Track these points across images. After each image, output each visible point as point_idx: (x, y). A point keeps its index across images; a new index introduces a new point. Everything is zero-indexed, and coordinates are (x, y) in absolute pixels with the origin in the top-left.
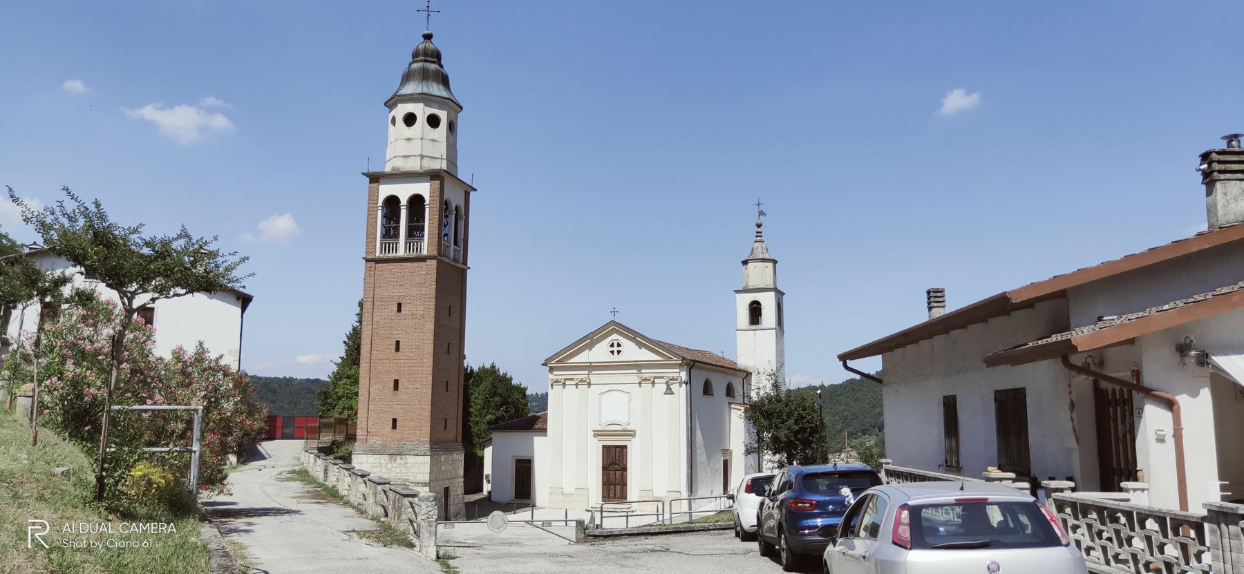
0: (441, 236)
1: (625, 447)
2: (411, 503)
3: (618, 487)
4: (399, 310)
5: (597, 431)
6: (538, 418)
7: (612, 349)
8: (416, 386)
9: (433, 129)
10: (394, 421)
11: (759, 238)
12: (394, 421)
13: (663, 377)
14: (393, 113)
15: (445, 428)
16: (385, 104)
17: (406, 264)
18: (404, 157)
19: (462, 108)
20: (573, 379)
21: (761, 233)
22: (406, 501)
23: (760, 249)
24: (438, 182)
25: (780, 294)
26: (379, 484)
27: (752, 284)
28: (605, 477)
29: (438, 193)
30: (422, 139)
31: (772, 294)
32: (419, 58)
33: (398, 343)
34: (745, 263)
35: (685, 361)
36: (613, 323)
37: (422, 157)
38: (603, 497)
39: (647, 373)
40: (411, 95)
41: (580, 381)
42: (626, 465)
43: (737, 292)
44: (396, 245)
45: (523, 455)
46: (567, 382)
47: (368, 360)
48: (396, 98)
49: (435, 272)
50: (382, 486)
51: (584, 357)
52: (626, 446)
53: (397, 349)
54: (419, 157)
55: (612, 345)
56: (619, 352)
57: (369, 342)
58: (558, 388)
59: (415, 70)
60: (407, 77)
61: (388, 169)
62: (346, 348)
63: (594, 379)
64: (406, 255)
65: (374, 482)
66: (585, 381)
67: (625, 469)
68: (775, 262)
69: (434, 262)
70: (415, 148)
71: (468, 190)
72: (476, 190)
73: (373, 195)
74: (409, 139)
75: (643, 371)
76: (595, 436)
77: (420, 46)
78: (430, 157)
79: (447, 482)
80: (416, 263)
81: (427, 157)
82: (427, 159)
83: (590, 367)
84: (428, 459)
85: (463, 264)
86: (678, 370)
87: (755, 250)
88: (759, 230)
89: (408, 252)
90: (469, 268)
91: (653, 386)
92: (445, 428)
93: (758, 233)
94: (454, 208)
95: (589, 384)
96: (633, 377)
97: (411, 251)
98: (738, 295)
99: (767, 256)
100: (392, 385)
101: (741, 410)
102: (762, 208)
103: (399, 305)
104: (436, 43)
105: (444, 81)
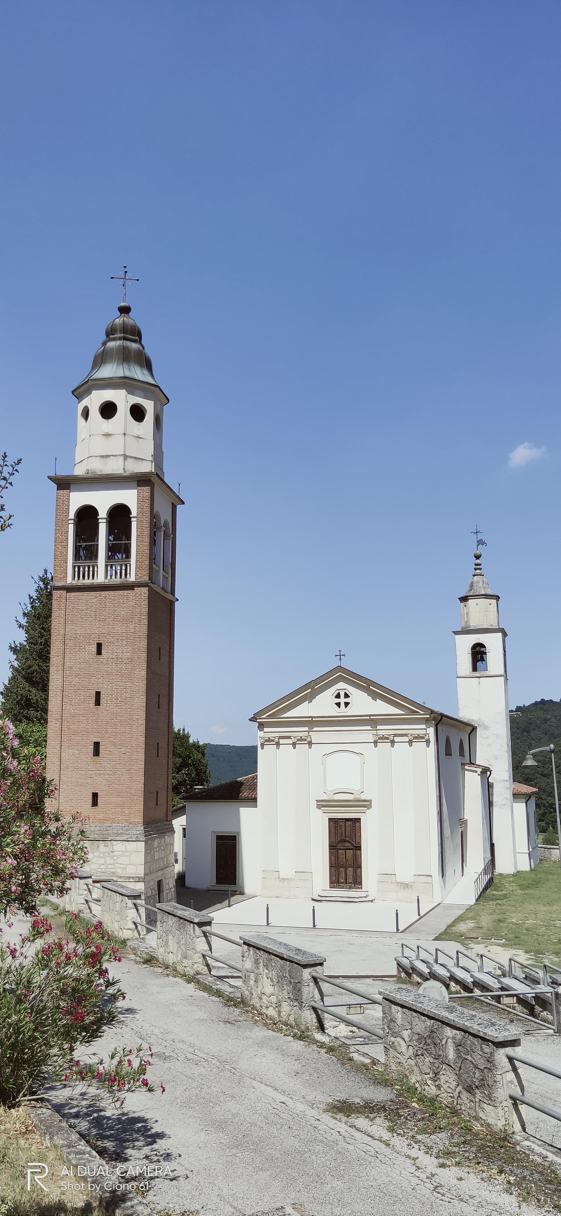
0: (152, 559)
1: (358, 820)
2: (511, 1059)
3: (350, 870)
4: (99, 652)
5: (322, 801)
6: (241, 784)
7: (338, 700)
8: (123, 750)
9: (137, 423)
10: (95, 796)
11: (478, 571)
12: (95, 796)
13: (406, 735)
14: (85, 402)
15: (157, 804)
16: (73, 392)
17: (107, 593)
18: (102, 457)
19: (168, 400)
20: (289, 737)
21: (480, 565)
22: (501, 1055)
23: (481, 584)
24: (146, 490)
25: (505, 635)
26: (305, 966)
27: (474, 623)
28: (333, 858)
29: (147, 504)
30: (125, 434)
31: (500, 635)
32: (116, 336)
33: (98, 694)
34: (464, 599)
35: (433, 715)
36: (340, 668)
37: (126, 457)
38: (331, 882)
39: (384, 730)
40: (111, 378)
41: (298, 740)
42: (360, 843)
43: (456, 633)
44: (93, 569)
45: (226, 829)
46: (282, 741)
47: (58, 717)
48: (90, 383)
49: (146, 602)
50: (309, 970)
51: (303, 710)
52: (360, 819)
53: (98, 703)
54: (122, 458)
55: (338, 696)
56: (347, 704)
57: (59, 693)
58: (270, 748)
59: (112, 350)
60: (100, 359)
61: (79, 471)
62: (3, 700)
63: (315, 737)
64: (106, 581)
65: (282, 958)
66: (305, 740)
67: (359, 848)
68: (497, 598)
69: (145, 590)
70: (116, 446)
71: (176, 501)
72: (183, 503)
73: (62, 506)
74: (107, 435)
75: (379, 727)
76: (319, 807)
77: (117, 320)
78: (135, 458)
79: (160, 873)
80: (121, 592)
81: (131, 457)
82: (132, 459)
83: (311, 723)
84: (141, 846)
85: (171, 594)
86: (424, 726)
87: (475, 585)
88: (478, 561)
89: (109, 577)
90: (178, 600)
91: (393, 746)
92: (157, 804)
93: (476, 565)
94: (162, 525)
95: (310, 743)
96: (367, 734)
97: (114, 577)
98: (458, 637)
99: (489, 592)
100: (91, 748)
101: (476, 772)
102: (480, 536)
103: (99, 646)
104: (134, 319)
105: (147, 365)
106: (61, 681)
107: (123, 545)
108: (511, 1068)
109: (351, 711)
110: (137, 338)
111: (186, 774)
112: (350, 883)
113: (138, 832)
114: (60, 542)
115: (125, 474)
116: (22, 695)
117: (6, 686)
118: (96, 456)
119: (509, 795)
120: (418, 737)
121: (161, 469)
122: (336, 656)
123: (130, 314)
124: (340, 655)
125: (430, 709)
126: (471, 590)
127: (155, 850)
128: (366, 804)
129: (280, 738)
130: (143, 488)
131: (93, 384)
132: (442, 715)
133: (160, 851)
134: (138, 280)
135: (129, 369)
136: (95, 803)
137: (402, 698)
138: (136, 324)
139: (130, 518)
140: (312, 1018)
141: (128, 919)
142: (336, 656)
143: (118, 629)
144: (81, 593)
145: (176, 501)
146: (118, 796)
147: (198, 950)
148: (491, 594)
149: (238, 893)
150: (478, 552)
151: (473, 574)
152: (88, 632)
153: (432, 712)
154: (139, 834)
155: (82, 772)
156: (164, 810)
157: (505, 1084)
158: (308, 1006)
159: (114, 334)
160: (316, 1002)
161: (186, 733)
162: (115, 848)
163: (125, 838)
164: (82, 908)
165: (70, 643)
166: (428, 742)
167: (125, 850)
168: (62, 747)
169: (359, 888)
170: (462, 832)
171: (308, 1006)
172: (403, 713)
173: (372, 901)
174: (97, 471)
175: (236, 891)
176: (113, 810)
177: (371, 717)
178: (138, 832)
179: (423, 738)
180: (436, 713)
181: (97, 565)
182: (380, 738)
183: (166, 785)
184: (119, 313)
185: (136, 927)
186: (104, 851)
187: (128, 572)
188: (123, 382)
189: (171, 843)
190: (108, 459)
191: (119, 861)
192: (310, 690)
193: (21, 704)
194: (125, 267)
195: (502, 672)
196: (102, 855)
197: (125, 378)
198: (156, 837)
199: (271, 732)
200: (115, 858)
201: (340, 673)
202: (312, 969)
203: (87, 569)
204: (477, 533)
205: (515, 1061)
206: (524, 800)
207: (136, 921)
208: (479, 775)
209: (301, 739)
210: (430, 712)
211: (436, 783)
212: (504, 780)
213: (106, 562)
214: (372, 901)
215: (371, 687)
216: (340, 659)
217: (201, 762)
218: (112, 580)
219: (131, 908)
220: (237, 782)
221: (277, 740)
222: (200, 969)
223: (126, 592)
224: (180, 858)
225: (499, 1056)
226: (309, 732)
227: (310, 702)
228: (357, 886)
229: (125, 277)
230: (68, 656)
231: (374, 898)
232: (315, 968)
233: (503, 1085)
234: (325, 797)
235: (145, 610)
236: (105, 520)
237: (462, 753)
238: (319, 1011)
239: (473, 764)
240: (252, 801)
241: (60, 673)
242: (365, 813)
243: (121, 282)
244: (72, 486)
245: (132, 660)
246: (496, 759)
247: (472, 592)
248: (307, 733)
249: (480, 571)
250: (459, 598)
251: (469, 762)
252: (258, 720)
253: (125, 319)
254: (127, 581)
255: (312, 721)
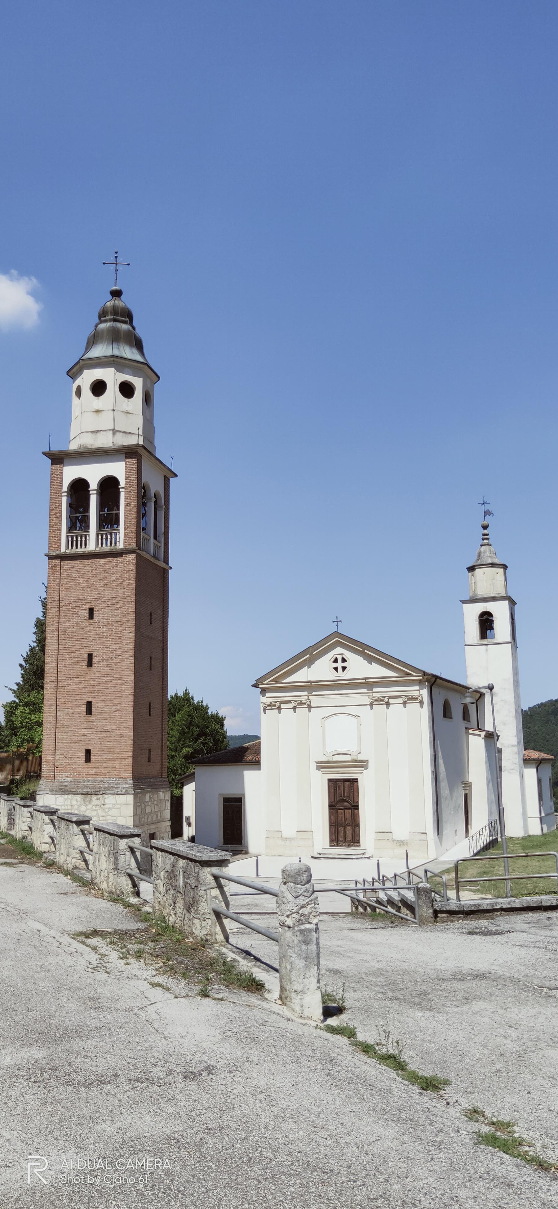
1: (356, 780)
2: (216, 878)
3: (349, 829)
4: (91, 616)
5: (321, 762)
7: (335, 665)
8: (113, 709)
9: (126, 399)
10: (88, 752)
11: (485, 541)
12: (88, 752)
13: (400, 697)
14: (78, 382)
15: (149, 761)
16: (68, 373)
17: (98, 560)
18: (93, 432)
19: (159, 377)
20: (289, 702)
21: (487, 535)
22: (207, 874)
23: (488, 553)
24: (133, 462)
25: (512, 603)
26: (122, 837)
27: (481, 592)
28: (332, 817)
29: (134, 475)
30: (114, 410)
31: (506, 603)
32: (107, 318)
33: (90, 656)
34: (471, 569)
35: (426, 677)
36: (336, 634)
37: (115, 431)
38: (331, 841)
39: (380, 692)
40: (100, 358)
41: (298, 704)
42: (358, 802)
43: (464, 602)
44: (86, 538)
45: (231, 792)
46: (283, 706)
47: (54, 678)
48: (81, 363)
49: (134, 568)
50: (125, 841)
51: (302, 675)
52: (357, 779)
53: (90, 664)
54: (111, 432)
55: (336, 661)
56: (344, 668)
57: (55, 656)
58: (272, 713)
59: (103, 331)
60: (93, 340)
61: (73, 446)
62: (22, 672)
63: (315, 701)
64: (97, 549)
65: (111, 834)
66: (305, 704)
67: (356, 807)
68: (505, 567)
69: (132, 557)
70: (106, 422)
71: (168, 475)
72: (176, 476)
73: (57, 479)
74: (98, 411)
75: (374, 690)
76: (319, 768)
77: (109, 303)
78: (124, 432)
79: (153, 826)
80: (111, 559)
81: (120, 432)
82: (121, 434)
83: (310, 687)
84: (130, 798)
85: (164, 562)
86: (417, 688)
87: (482, 555)
88: (486, 532)
89: (100, 546)
90: (171, 568)
91: (388, 708)
92: (149, 761)
93: (484, 535)
94: (153, 495)
95: (310, 707)
96: (362, 697)
97: (104, 545)
98: (465, 606)
99: (496, 561)
100: (84, 707)
101: (480, 735)
102: (487, 507)
103: (91, 611)
104: (126, 302)
105: (138, 344)
106: (56, 644)
107: (114, 515)
108: (216, 885)
109: (349, 675)
110: (128, 319)
111: (202, 743)
112: (349, 841)
113: (127, 786)
114: (55, 513)
115: (113, 447)
116: (37, 666)
117: (24, 658)
118: (88, 432)
119: (517, 760)
120: (412, 699)
121: (152, 443)
122: (334, 622)
123: (121, 297)
124: (337, 621)
125: (422, 671)
126: (478, 560)
127: (146, 804)
128: (363, 765)
129: (281, 702)
130: (130, 460)
131: (85, 364)
132: (436, 677)
133: (152, 805)
134: (129, 264)
135: (119, 349)
136: (88, 759)
137: (395, 660)
138: (126, 306)
139: (119, 489)
140: (127, 884)
141: (45, 833)
142: (334, 622)
143: (109, 594)
144: (74, 562)
145: (168, 475)
146: (109, 752)
147: (76, 847)
148: (498, 563)
149: (243, 852)
150: (486, 523)
151: (481, 543)
152: (81, 597)
153: (425, 673)
154: (128, 788)
155: (76, 730)
156: (158, 767)
157: (208, 899)
158: (124, 873)
159: (105, 317)
160: (131, 870)
161: (205, 705)
162: (107, 801)
163: (116, 791)
164: (26, 834)
165: (64, 609)
166: (421, 703)
167: (115, 802)
168: (58, 707)
169: (357, 846)
170: (466, 796)
171: (124, 873)
172: (396, 675)
173: (369, 858)
174: (88, 445)
175: (242, 851)
176: (105, 766)
177: (367, 680)
178: (127, 786)
179: (416, 699)
180: (429, 675)
181: (89, 534)
182: (376, 700)
183: (160, 744)
184: (111, 297)
185: (53, 841)
186: (96, 804)
187: (118, 540)
188: (110, 361)
189: (166, 799)
190: (98, 434)
191: (110, 813)
192: (308, 656)
193: (38, 675)
194: (116, 253)
195: (509, 638)
196: (94, 808)
197: (113, 356)
198: (148, 792)
199: (272, 697)
200: (106, 810)
201: (337, 639)
202: (129, 839)
203: (79, 538)
204: (484, 504)
205: (221, 879)
206: (535, 766)
207: (52, 835)
208: (483, 738)
209: (301, 703)
210: (422, 673)
211: (430, 743)
212: (513, 746)
213: (97, 531)
214: (369, 858)
215: (366, 651)
216: (337, 625)
217: (218, 732)
218: (102, 548)
219: (48, 824)
220: (244, 747)
221: (278, 704)
222: (77, 864)
223: (115, 559)
224: (193, 821)
225: (204, 874)
226: (308, 696)
227: (309, 667)
228: (356, 844)
229: (116, 261)
230: (62, 620)
231: (371, 855)
232: (132, 839)
233: (206, 900)
234: (324, 759)
235: (133, 575)
236: (95, 492)
237: (466, 716)
238: (135, 878)
239: (481, 729)
240: (256, 764)
241: (56, 637)
242: (362, 773)
243: (113, 267)
244: (65, 461)
245: (121, 623)
246: (505, 724)
247: (479, 561)
248: (307, 697)
249: (487, 541)
250: (467, 568)
251: (476, 727)
252: (260, 686)
253: (116, 302)
254: (116, 549)
255: (311, 686)
